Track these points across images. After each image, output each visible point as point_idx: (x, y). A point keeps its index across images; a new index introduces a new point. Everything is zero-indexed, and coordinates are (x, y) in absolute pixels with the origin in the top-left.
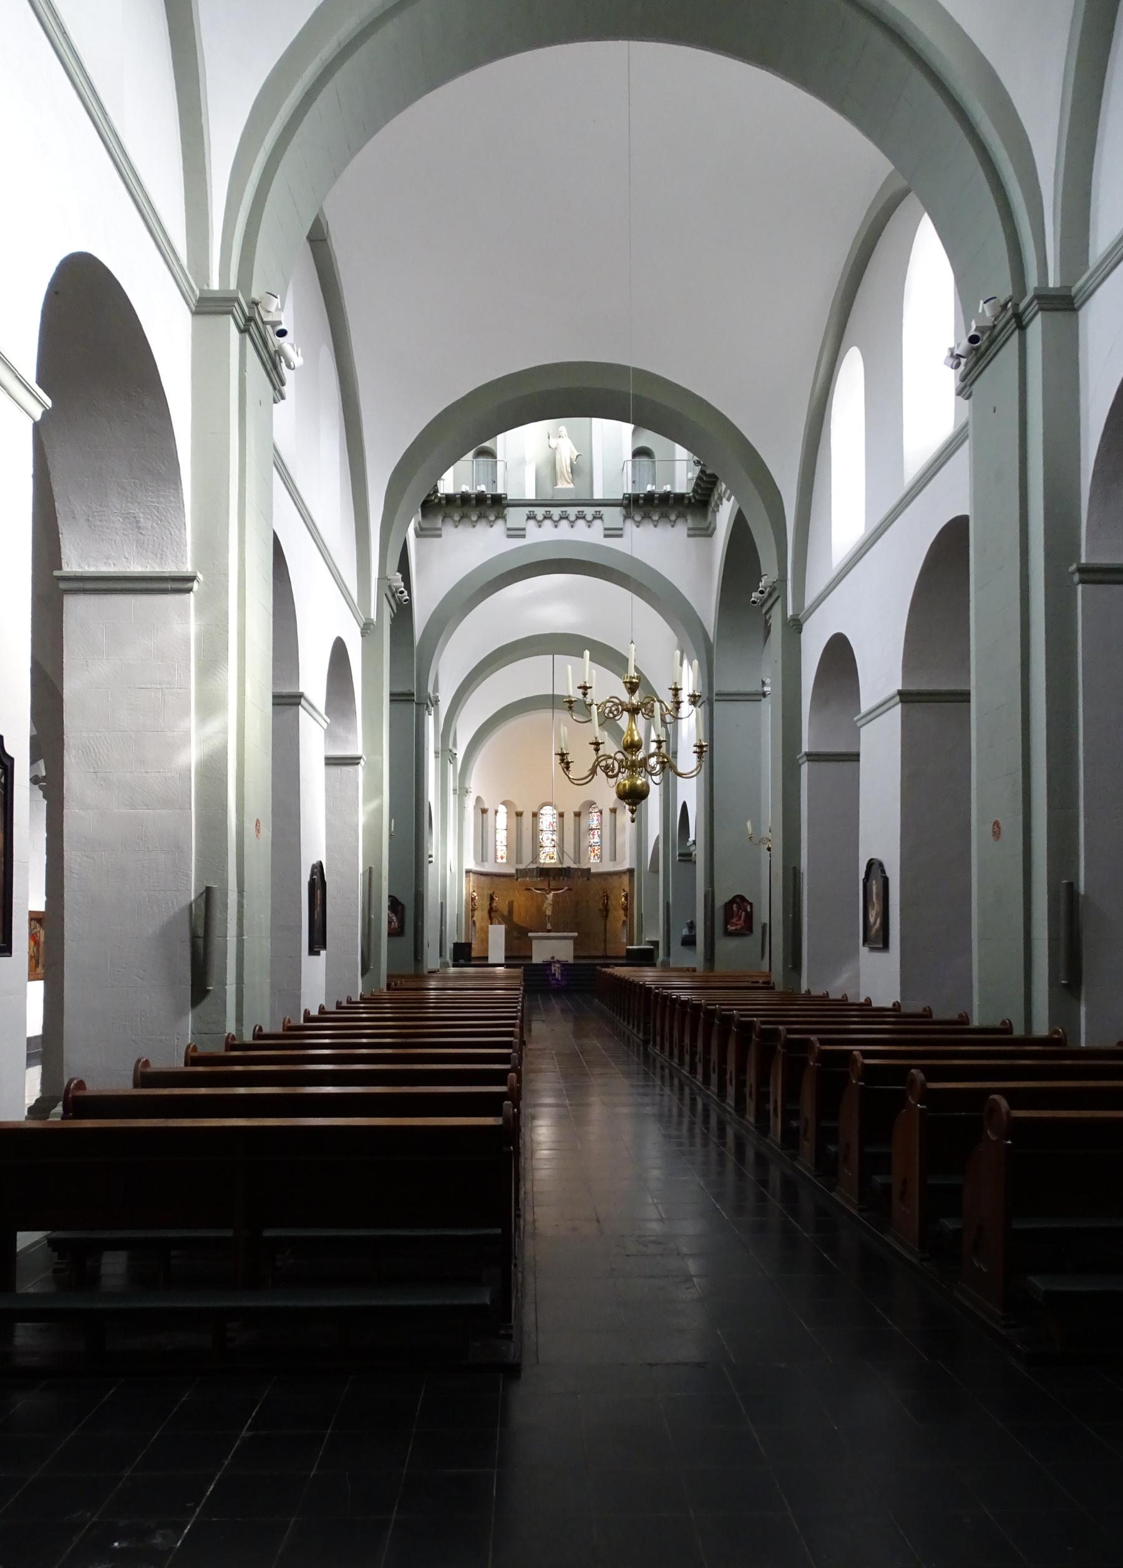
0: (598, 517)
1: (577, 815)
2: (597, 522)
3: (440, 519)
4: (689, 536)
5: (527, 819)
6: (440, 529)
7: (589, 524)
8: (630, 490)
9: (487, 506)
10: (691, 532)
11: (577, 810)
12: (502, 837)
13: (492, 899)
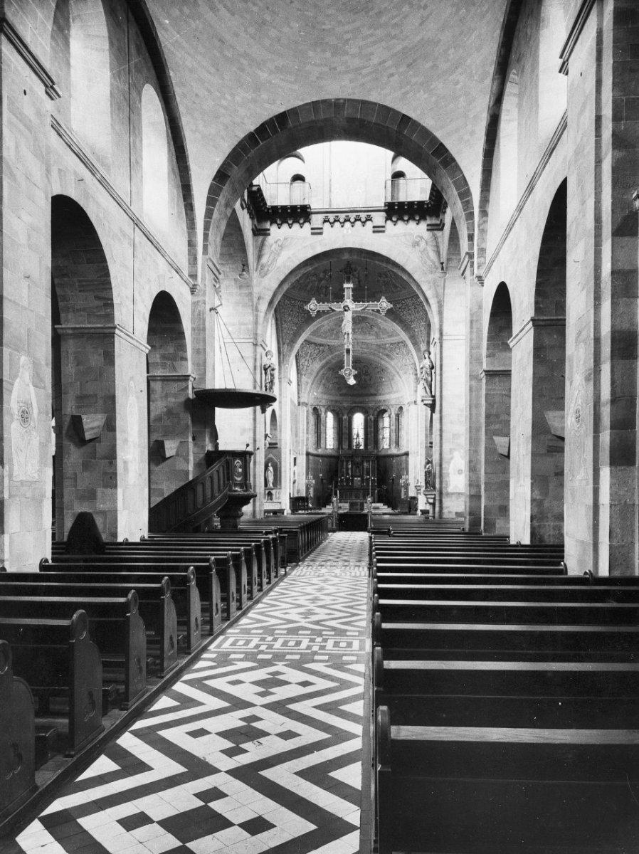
0: (369, 219)
2: (369, 223)
3: (269, 223)
4: (428, 230)
6: (269, 230)
7: (364, 223)
8: (389, 200)
9: (299, 214)
10: (430, 228)
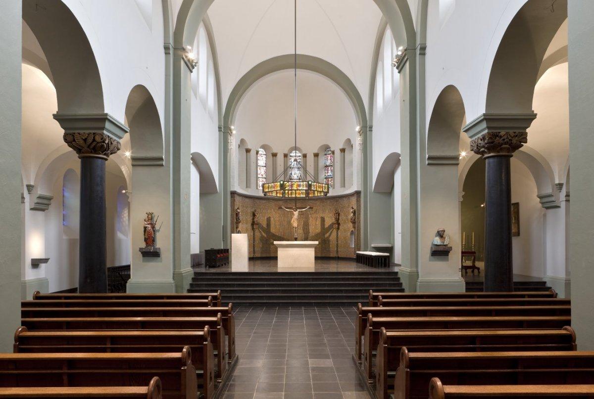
1: (316, 155)
5: (280, 158)
11: (316, 152)
12: (262, 171)
13: (254, 215)
